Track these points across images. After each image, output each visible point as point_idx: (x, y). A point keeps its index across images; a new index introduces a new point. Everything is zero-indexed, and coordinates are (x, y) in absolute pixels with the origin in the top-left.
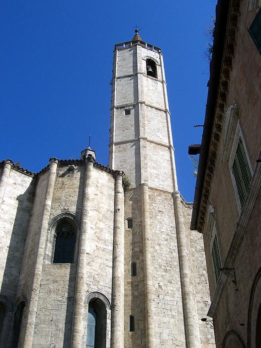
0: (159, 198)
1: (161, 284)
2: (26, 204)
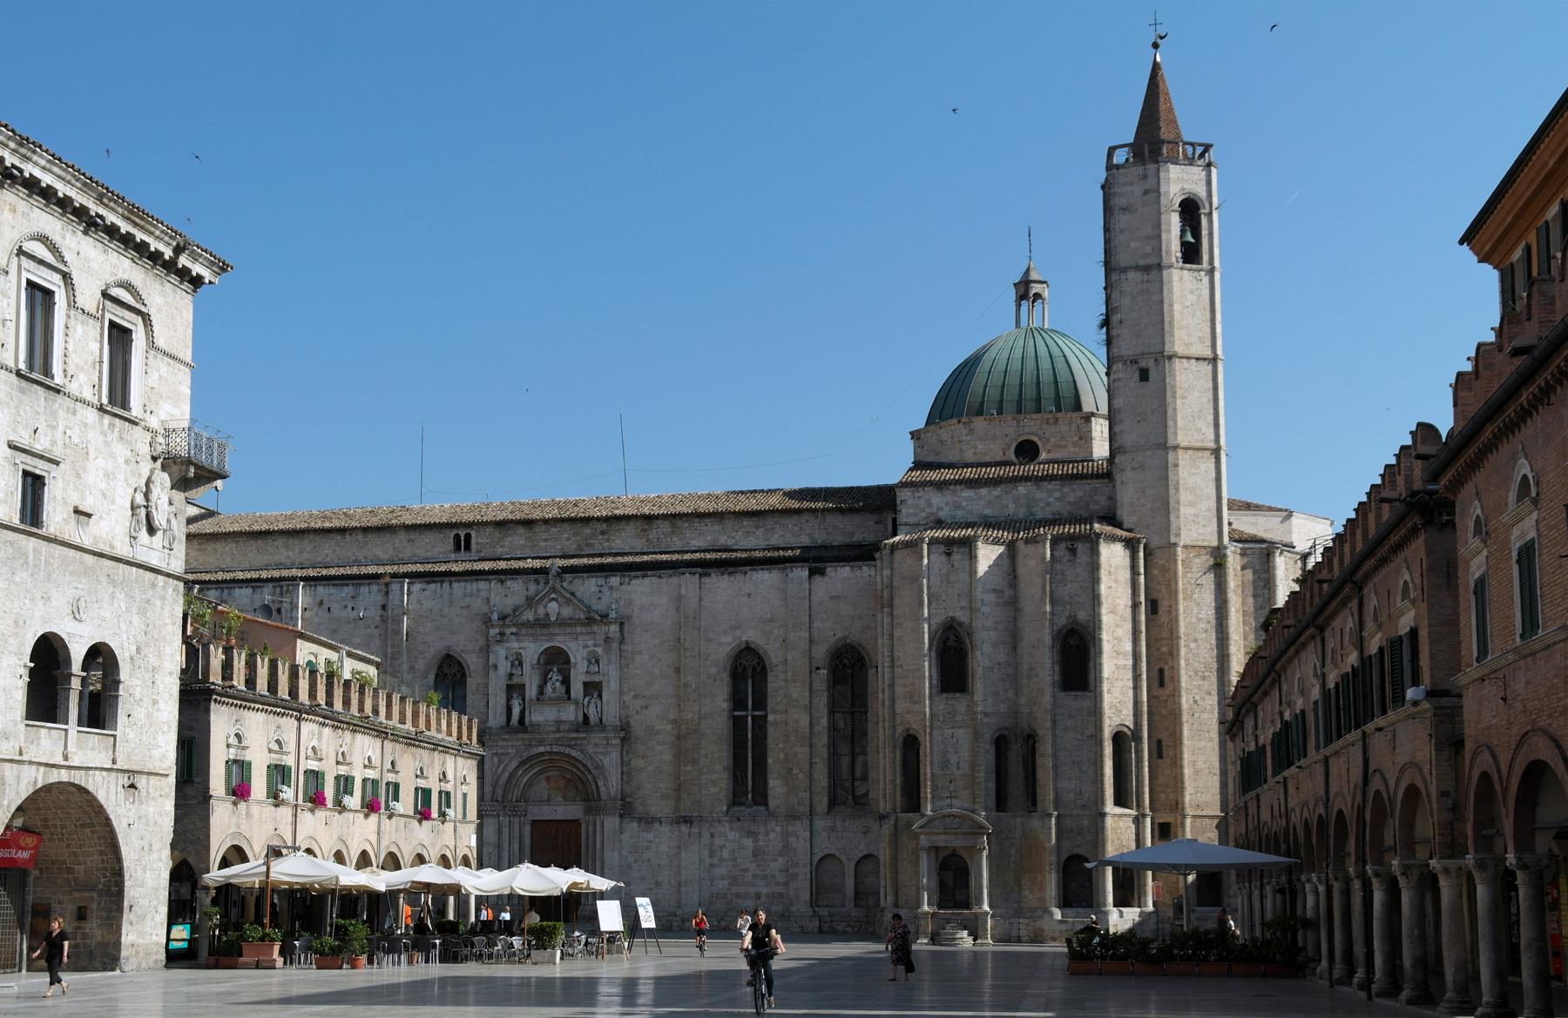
0: (1197, 560)
1: (1197, 698)
2: (1008, 592)
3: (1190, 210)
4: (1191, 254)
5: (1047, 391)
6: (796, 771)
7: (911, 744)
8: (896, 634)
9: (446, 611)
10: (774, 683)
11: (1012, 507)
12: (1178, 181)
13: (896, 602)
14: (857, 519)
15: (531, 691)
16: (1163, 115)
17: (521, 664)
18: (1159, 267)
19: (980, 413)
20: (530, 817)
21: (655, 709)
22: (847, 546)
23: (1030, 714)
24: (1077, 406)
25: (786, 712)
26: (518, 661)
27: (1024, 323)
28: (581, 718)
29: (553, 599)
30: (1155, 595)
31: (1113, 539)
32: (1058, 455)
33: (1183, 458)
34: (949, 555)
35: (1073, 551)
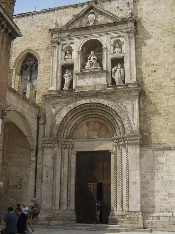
9: (29, 30)
15: (77, 68)
20: (76, 150)
21: (161, 72)
28: (110, 82)
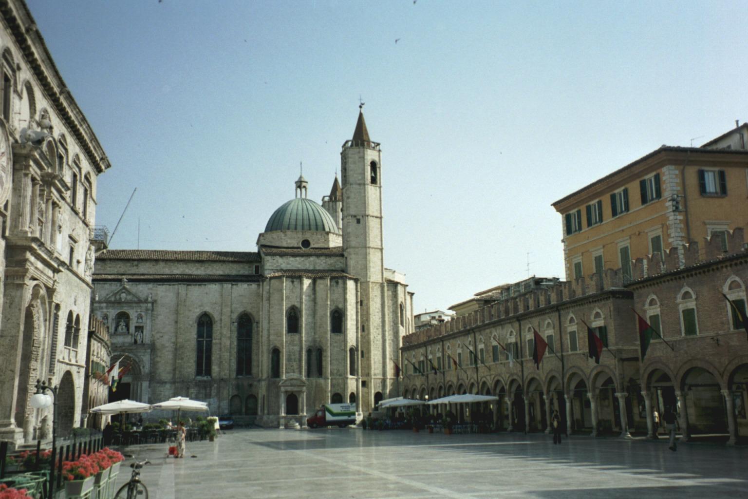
2: (313, 296)
3: (374, 166)
4: (374, 180)
5: (313, 222)
6: (224, 362)
7: (276, 353)
8: (271, 310)
10: (216, 328)
11: (308, 265)
12: (370, 155)
13: (271, 299)
14: (242, 265)
16: (364, 132)
17: (107, 318)
18: (364, 184)
19: (288, 229)
21: (166, 337)
22: (237, 276)
23: (320, 341)
24: (324, 229)
25: (221, 339)
26: (106, 317)
27: (299, 196)
28: (133, 341)
29: (124, 292)
30: (362, 299)
31: (350, 279)
32: (316, 246)
33: (372, 251)
34: (293, 282)
35: (337, 283)
